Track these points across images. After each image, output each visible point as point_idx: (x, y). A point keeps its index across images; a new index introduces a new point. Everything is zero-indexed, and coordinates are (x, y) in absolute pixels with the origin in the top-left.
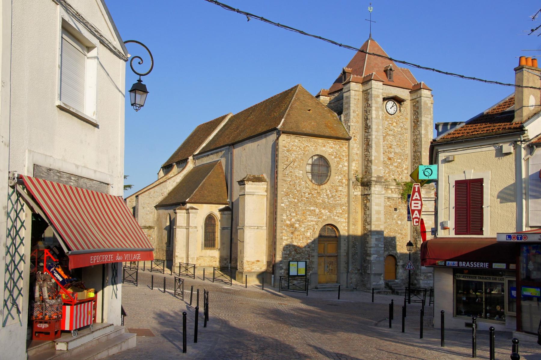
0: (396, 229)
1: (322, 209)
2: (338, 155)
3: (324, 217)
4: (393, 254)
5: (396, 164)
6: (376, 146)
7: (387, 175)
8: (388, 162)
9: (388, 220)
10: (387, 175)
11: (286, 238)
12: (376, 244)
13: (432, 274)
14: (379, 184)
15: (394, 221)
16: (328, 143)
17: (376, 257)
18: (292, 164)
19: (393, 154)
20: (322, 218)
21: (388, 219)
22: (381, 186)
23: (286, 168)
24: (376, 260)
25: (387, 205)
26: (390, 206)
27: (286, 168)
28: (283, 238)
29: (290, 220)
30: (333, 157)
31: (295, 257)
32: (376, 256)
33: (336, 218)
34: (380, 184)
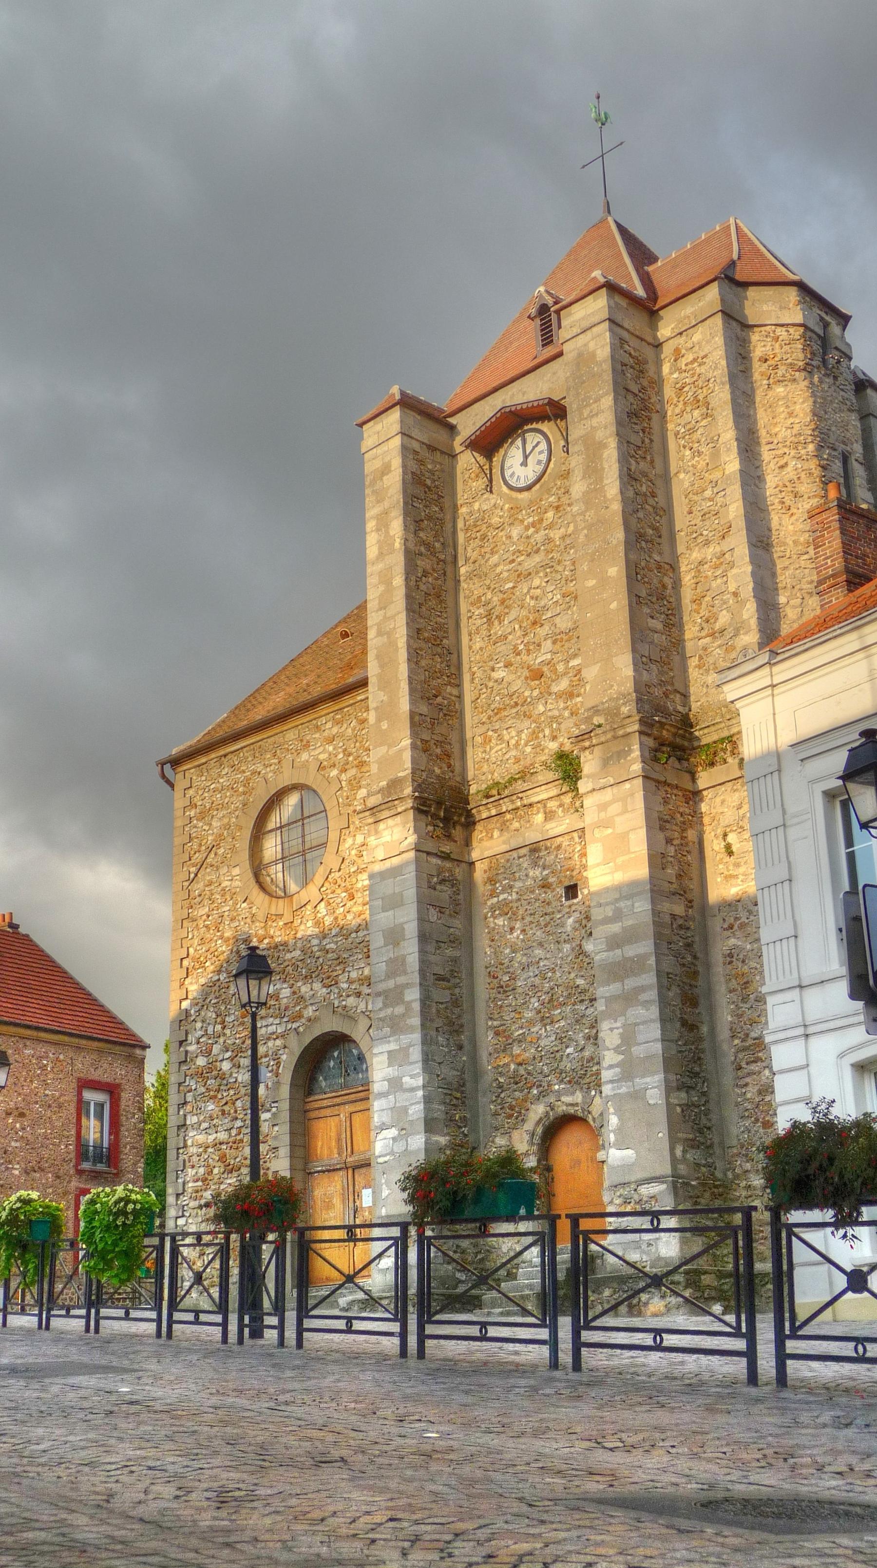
0: (580, 982)
1: (299, 984)
2: (351, 758)
3: (309, 1012)
4: (571, 1110)
5: (563, 685)
6: (382, 666)
7: (528, 749)
8: (527, 693)
9: (538, 952)
10: (528, 749)
11: (195, 1119)
12: (389, 1080)
13: (664, 1186)
14: (386, 814)
15: (567, 947)
16: (318, 728)
17: (394, 1139)
18: (212, 855)
19: (548, 645)
20: (300, 1016)
21: (541, 945)
22: (398, 819)
23: (196, 875)
24: (392, 1153)
25: (529, 882)
26: (545, 886)
27: (196, 875)
28: (188, 1122)
29: (209, 1053)
30: (334, 773)
31: (222, 1187)
32: (393, 1132)
33: (351, 1001)
34: (393, 812)
